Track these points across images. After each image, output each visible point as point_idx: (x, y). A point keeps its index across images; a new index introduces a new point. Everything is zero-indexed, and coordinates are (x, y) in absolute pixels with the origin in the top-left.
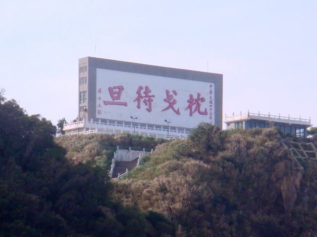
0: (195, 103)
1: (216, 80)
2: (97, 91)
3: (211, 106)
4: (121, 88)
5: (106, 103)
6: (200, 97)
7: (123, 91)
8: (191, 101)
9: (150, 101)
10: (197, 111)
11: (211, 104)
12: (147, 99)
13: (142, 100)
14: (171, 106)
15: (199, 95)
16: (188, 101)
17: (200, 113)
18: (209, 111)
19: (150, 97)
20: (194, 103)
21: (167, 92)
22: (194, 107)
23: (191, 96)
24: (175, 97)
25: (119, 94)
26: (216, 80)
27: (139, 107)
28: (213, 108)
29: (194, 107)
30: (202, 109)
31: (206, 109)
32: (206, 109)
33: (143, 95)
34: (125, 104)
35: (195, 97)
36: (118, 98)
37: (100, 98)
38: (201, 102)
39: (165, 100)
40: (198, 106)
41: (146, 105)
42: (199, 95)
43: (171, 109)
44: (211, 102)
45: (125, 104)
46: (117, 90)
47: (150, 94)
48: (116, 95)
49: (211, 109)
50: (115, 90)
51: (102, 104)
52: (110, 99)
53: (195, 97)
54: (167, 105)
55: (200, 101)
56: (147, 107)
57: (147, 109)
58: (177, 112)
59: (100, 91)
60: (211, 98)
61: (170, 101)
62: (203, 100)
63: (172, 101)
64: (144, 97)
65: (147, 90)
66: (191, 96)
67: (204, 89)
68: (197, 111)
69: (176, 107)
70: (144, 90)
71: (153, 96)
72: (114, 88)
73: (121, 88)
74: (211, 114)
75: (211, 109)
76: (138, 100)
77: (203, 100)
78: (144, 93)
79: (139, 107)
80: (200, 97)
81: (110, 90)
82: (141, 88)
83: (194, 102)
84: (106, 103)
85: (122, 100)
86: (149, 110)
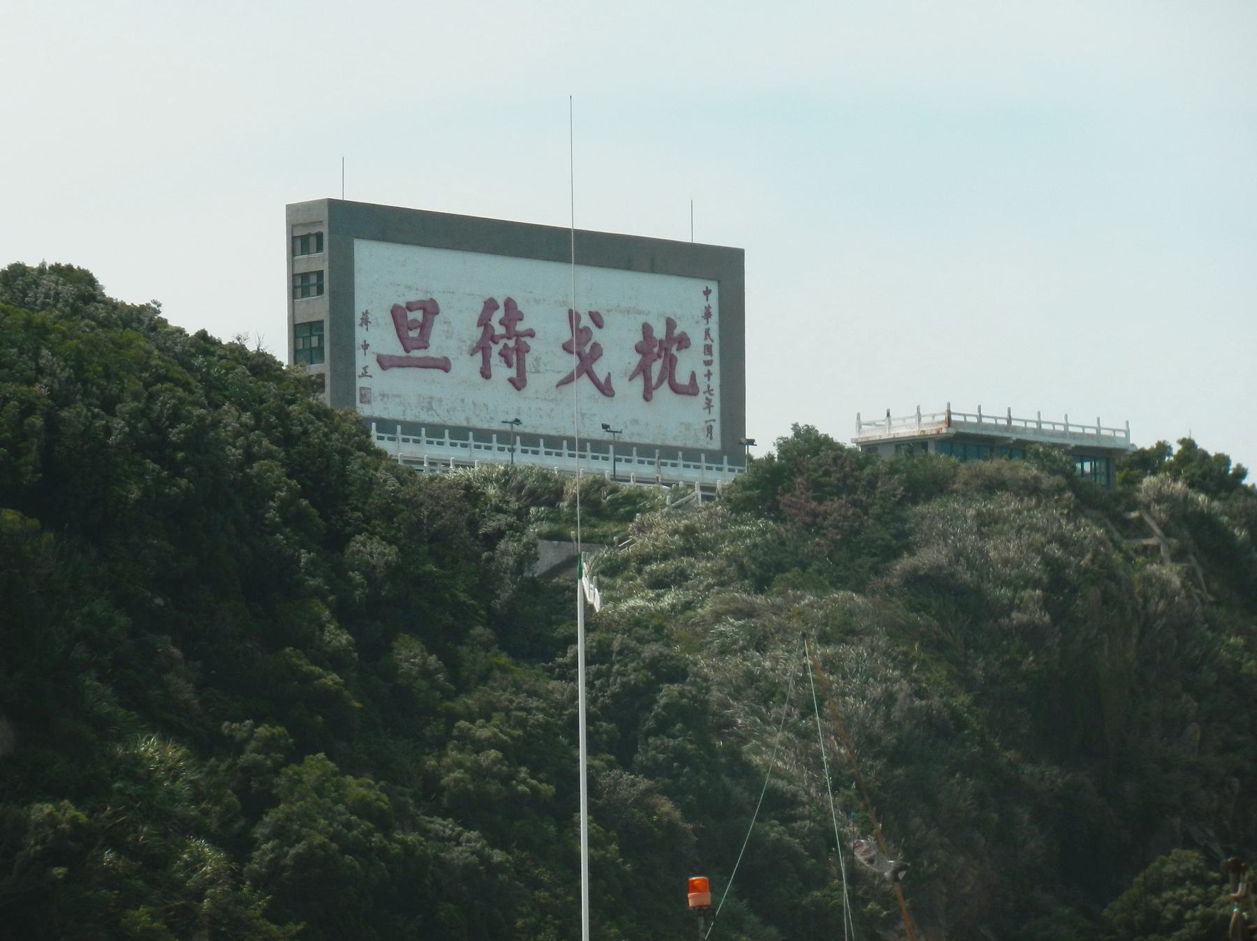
0: (659, 357)
3: (708, 363)
4: (430, 309)
6: (677, 332)
7: (437, 319)
9: (522, 350)
10: (666, 384)
11: (708, 358)
12: (511, 343)
13: (496, 349)
15: (670, 324)
16: (638, 349)
17: (676, 389)
18: (702, 382)
19: (519, 335)
21: (573, 317)
22: (656, 368)
23: (647, 330)
24: (597, 335)
25: (425, 327)
27: (486, 373)
28: (715, 368)
29: (656, 368)
30: (682, 378)
31: (693, 376)
32: (693, 376)
33: (499, 330)
35: (659, 332)
38: (679, 349)
39: (567, 348)
40: (671, 363)
41: (509, 365)
42: (670, 324)
44: (708, 349)
46: (418, 315)
47: (521, 327)
48: (414, 334)
49: (709, 375)
50: (411, 316)
51: (374, 368)
52: (396, 349)
53: (659, 332)
56: (512, 373)
57: (511, 380)
58: (606, 389)
59: (365, 321)
60: (707, 332)
61: (583, 350)
64: (502, 337)
65: (512, 312)
66: (647, 330)
68: (666, 384)
72: (410, 307)
73: (430, 309)
74: (709, 391)
75: (709, 375)
77: (683, 342)
79: (486, 373)
80: (677, 332)
81: (397, 314)
82: (490, 305)
83: (656, 350)
86: (518, 383)
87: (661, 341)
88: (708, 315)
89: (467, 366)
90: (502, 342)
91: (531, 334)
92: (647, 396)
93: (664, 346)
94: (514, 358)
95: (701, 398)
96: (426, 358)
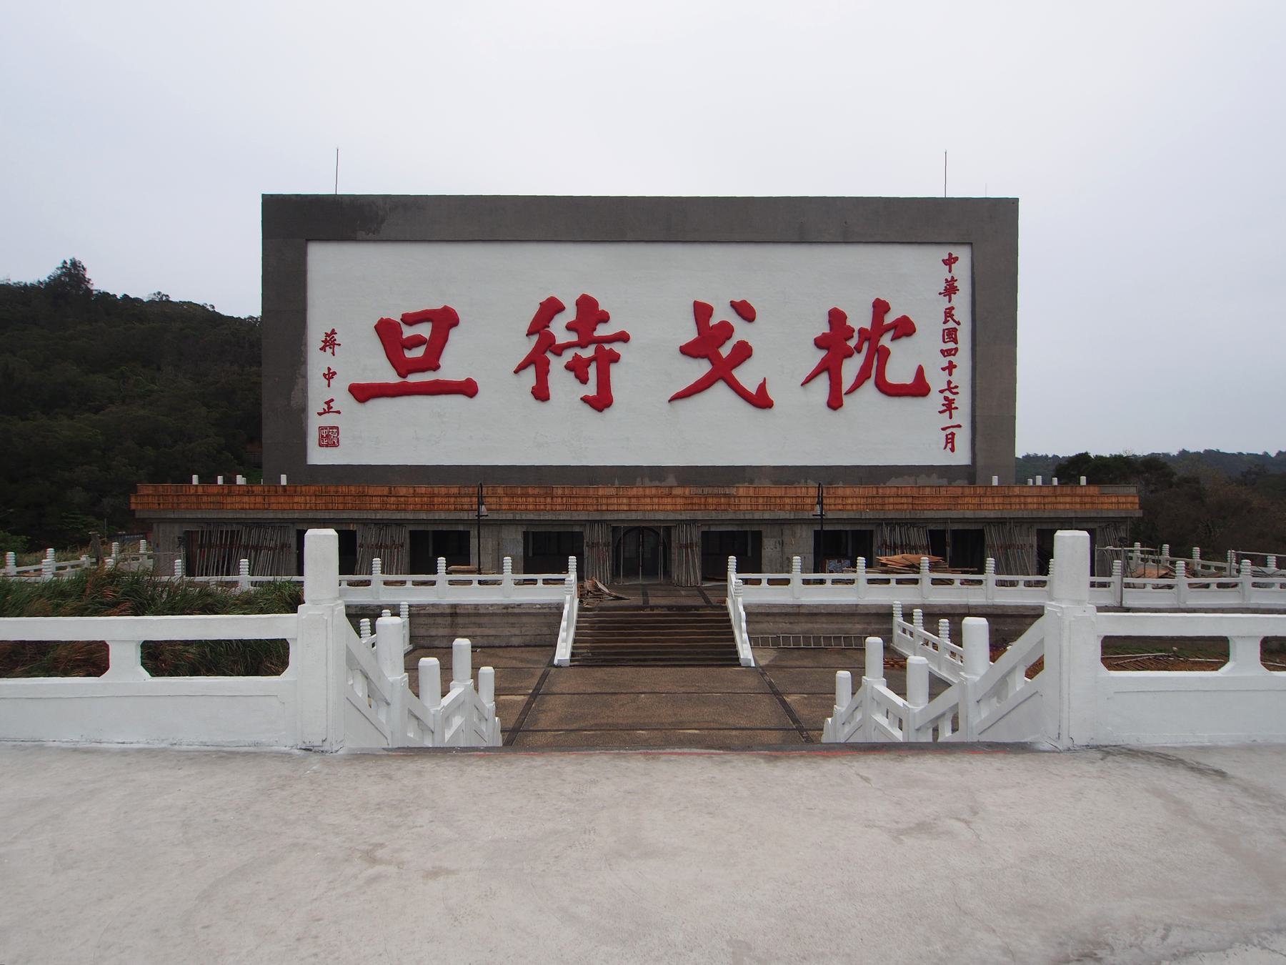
1: (981, 232)
2: (315, 337)
4: (445, 320)
5: (363, 393)
6: (889, 319)
7: (454, 334)
8: (835, 340)
9: (607, 360)
10: (870, 385)
11: (951, 345)
12: (588, 352)
13: (557, 365)
14: (722, 372)
15: (880, 307)
16: (820, 343)
17: (888, 390)
18: (936, 380)
20: (852, 350)
21: (702, 311)
23: (836, 317)
24: (742, 330)
25: (437, 345)
26: (981, 232)
27: (541, 393)
28: (963, 360)
30: (899, 372)
31: (920, 371)
32: (920, 371)
34: (468, 389)
35: (860, 319)
36: (431, 362)
37: (330, 375)
39: (688, 351)
41: (584, 380)
42: (880, 307)
43: (720, 389)
44: (951, 335)
45: (468, 389)
46: (425, 330)
47: (602, 331)
48: (418, 352)
49: (950, 368)
50: (408, 332)
51: (344, 401)
52: (391, 377)
53: (860, 319)
54: (701, 368)
55: (889, 335)
56: (591, 389)
57: (585, 400)
58: (760, 400)
59: (330, 342)
60: (949, 313)
61: (716, 349)
62: (905, 328)
63: (725, 351)
64: (570, 345)
65: (590, 313)
66: (836, 317)
67: (915, 280)
68: (870, 385)
69: (747, 376)
70: (570, 314)
71: (623, 337)
72: (411, 319)
73: (445, 320)
74: (950, 388)
76: (537, 361)
77: (905, 328)
78: (570, 327)
79: (541, 393)
80: (889, 319)
81: (387, 331)
82: (551, 308)
84: (363, 393)
85: (451, 368)
86: (601, 402)
87: (861, 331)
88: (950, 289)
89: (505, 388)
90: (568, 355)
91: (623, 337)
92: (835, 402)
93: (869, 337)
94: (592, 371)
95: (935, 400)
96: (437, 382)
